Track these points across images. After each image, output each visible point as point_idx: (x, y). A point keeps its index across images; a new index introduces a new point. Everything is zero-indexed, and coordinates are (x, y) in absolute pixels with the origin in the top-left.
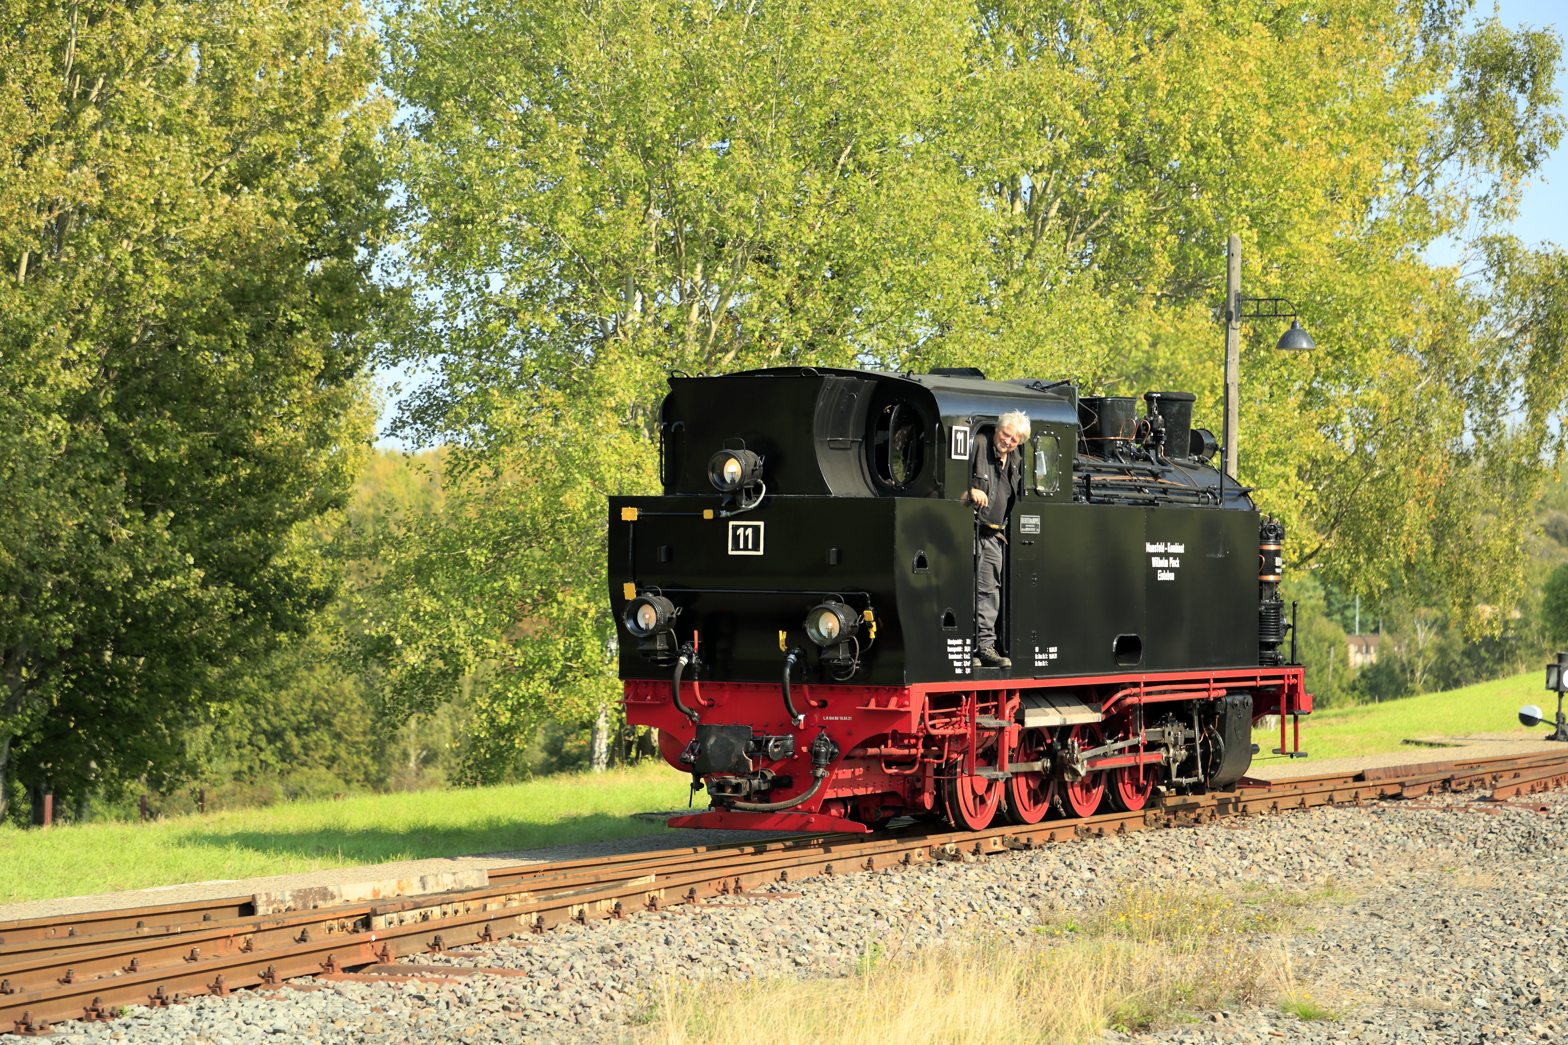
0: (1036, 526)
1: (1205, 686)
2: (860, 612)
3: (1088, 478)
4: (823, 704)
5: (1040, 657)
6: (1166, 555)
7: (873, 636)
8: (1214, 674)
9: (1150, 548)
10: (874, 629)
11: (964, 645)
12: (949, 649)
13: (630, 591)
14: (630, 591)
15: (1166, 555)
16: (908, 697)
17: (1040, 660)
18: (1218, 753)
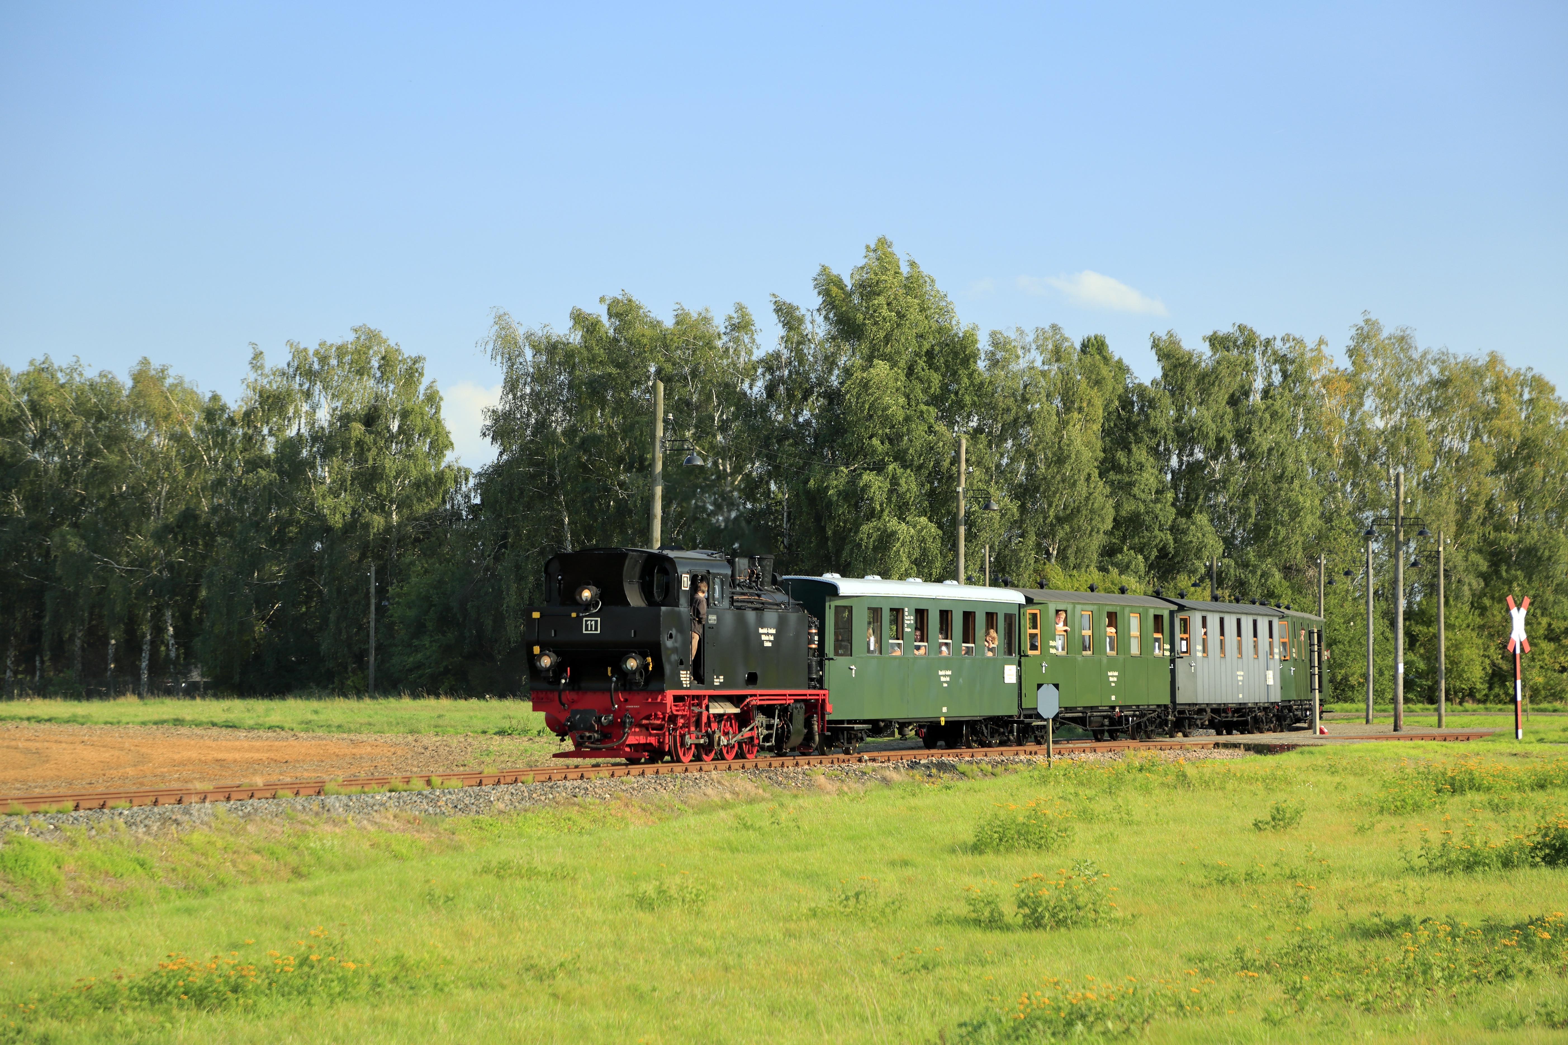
2: (645, 658)
4: (626, 700)
6: (767, 634)
8: (788, 692)
13: (537, 650)
14: (537, 650)
15: (767, 634)
17: (717, 682)
18: (789, 731)
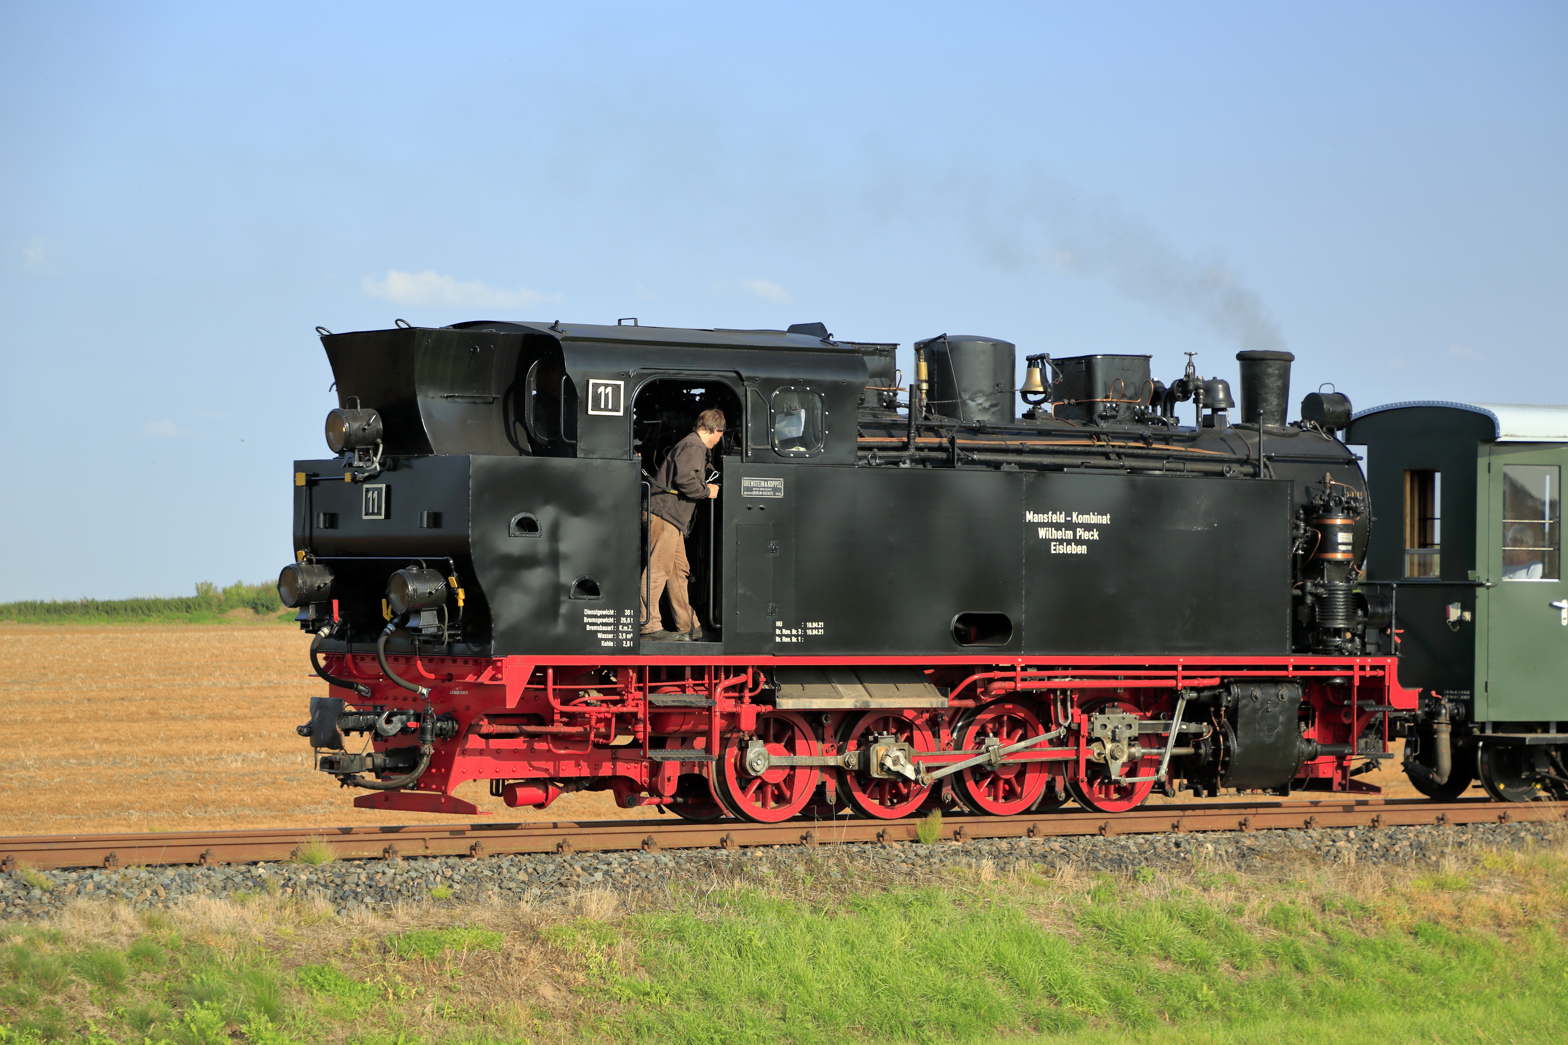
0: (775, 489)
3: (952, 441)
5: (787, 632)
7: (461, 604)
9: (1030, 517)
10: (461, 594)
11: (618, 616)
12: (586, 620)
15: (1070, 526)
16: (499, 670)
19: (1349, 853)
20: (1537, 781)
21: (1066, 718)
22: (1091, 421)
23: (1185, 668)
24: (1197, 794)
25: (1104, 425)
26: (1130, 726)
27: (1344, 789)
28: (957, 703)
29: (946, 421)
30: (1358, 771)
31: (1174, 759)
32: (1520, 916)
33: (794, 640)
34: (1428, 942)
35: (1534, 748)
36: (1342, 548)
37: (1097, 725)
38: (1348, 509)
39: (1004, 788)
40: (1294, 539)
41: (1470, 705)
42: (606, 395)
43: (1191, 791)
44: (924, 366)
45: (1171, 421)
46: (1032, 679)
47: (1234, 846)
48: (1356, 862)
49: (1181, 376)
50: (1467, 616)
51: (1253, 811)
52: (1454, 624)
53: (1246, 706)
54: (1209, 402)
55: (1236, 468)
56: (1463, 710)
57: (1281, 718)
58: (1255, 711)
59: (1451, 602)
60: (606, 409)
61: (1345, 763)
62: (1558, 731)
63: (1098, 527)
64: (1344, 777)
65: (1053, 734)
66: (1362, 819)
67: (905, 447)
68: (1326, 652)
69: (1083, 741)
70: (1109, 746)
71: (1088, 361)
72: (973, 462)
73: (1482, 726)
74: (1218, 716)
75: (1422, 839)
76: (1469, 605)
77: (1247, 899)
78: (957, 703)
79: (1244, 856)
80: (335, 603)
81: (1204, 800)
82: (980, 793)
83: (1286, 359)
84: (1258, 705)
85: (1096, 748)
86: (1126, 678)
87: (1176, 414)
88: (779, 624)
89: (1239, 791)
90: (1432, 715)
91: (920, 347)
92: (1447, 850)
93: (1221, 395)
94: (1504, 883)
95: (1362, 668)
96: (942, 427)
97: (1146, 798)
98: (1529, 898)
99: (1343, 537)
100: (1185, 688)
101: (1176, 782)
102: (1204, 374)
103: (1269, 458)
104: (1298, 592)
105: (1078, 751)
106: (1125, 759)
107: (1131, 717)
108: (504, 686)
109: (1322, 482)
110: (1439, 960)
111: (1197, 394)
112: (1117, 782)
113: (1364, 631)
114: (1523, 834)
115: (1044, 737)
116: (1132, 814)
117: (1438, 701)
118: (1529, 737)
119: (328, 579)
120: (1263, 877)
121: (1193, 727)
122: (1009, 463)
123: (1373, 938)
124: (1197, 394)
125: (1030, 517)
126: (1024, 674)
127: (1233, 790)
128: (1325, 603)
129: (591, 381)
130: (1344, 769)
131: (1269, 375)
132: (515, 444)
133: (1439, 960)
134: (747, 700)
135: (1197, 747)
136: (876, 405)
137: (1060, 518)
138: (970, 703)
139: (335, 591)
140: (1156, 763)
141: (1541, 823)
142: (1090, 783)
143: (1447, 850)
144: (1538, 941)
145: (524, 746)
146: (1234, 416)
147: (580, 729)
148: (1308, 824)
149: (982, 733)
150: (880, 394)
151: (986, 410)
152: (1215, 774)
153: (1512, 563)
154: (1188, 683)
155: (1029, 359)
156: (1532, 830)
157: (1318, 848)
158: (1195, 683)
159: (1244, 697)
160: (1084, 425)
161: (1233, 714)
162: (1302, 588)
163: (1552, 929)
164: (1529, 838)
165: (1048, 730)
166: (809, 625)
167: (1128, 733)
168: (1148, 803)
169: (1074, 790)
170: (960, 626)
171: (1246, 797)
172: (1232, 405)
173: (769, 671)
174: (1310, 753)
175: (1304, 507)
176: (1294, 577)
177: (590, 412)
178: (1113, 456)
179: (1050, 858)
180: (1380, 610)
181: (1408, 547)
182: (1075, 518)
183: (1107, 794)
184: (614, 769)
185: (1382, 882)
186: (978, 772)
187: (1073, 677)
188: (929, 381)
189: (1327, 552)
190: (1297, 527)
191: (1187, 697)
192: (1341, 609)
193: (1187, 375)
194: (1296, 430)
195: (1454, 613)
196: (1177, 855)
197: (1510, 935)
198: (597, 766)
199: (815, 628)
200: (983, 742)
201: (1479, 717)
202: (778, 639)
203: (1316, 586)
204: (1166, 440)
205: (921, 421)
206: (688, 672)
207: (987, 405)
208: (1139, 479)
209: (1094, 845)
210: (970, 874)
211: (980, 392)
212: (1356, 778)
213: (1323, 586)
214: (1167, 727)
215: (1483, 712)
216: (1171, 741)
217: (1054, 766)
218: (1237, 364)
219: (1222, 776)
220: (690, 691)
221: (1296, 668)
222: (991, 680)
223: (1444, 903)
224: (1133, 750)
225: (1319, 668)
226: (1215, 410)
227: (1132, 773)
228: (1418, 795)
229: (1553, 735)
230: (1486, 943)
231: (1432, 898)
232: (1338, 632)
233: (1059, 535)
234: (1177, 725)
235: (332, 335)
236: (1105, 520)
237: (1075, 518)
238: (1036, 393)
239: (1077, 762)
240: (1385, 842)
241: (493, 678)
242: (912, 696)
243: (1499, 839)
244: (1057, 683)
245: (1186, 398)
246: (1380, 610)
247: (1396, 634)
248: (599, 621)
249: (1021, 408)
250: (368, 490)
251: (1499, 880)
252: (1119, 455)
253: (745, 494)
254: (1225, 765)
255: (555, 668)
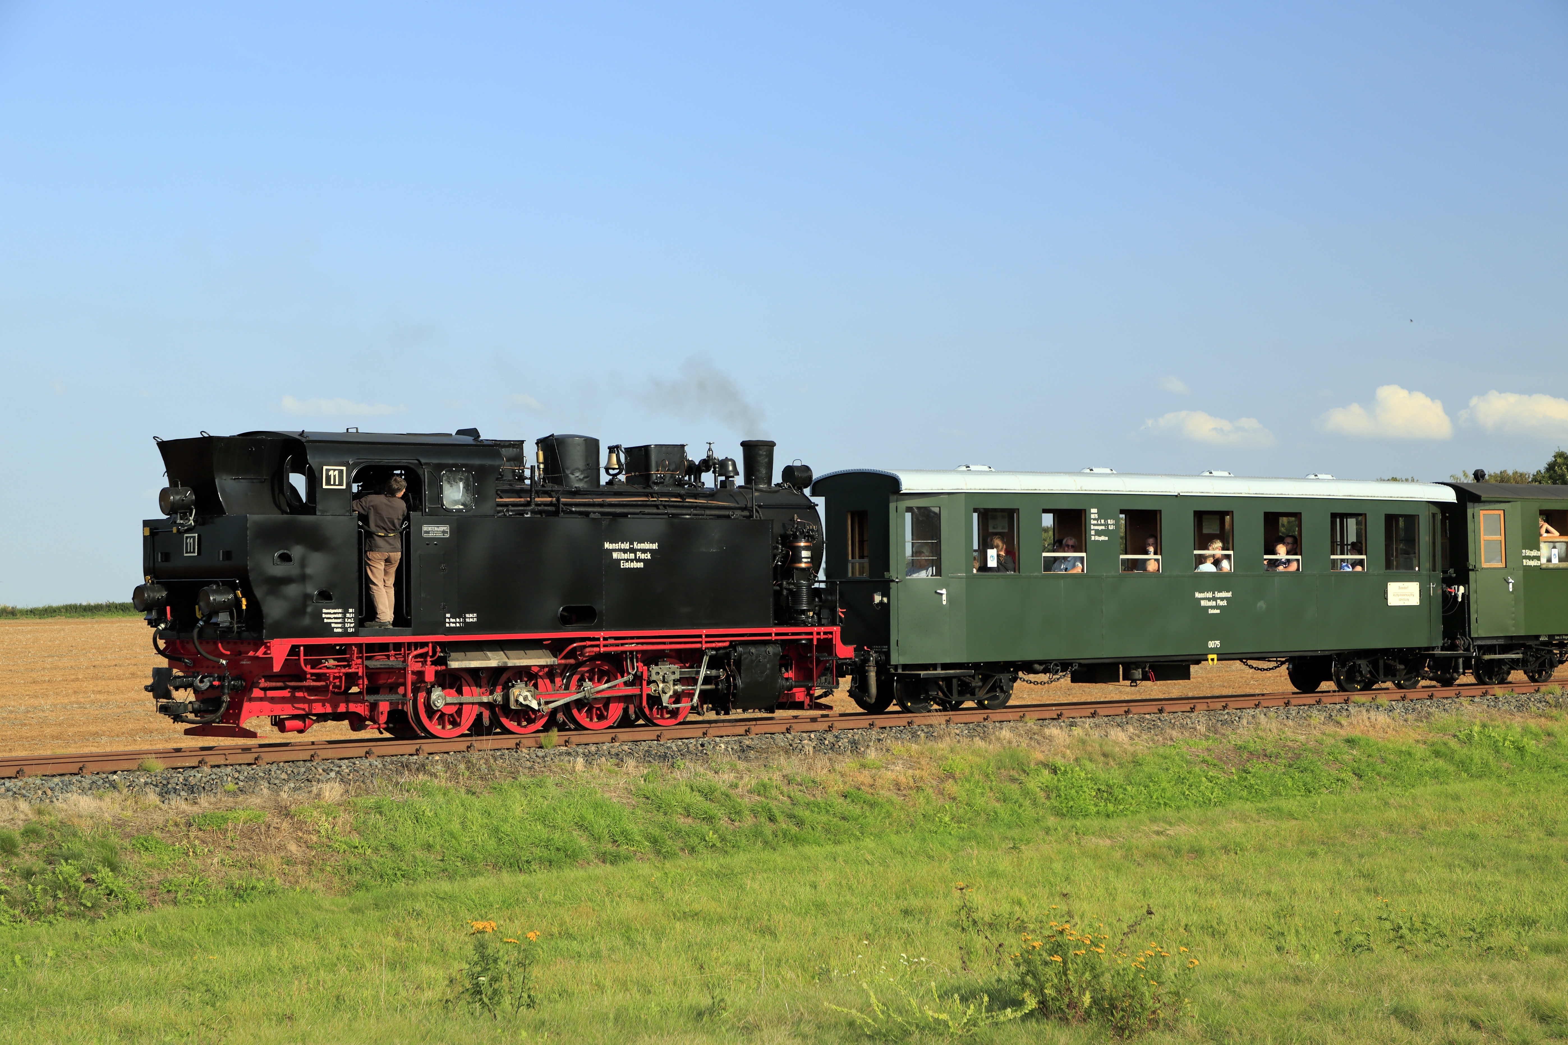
0: (444, 532)
1: (700, 639)
3: (558, 500)
7: (244, 607)
9: (607, 545)
11: (344, 613)
12: (324, 616)
15: (633, 551)
16: (268, 648)
19: (809, 747)
20: (931, 700)
21: (633, 669)
22: (648, 486)
23: (707, 636)
24: (718, 714)
25: (656, 488)
26: (674, 673)
27: (811, 708)
28: (563, 661)
29: (556, 488)
30: (820, 697)
31: (702, 692)
32: (911, 783)
33: (458, 625)
34: (853, 801)
35: (928, 680)
36: (804, 560)
37: (653, 673)
38: (808, 536)
39: (596, 713)
40: (775, 556)
41: (888, 654)
42: (335, 476)
43: (714, 712)
44: (541, 453)
45: (700, 484)
46: (612, 645)
47: (738, 744)
48: (814, 752)
49: (705, 457)
50: (885, 600)
51: (754, 723)
52: (878, 604)
53: (746, 658)
54: (723, 472)
55: (738, 513)
56: (883, 658)
57: (768, 666)
58: (752, 661)
59: (876, 592)
60: (334, 484)
61: (811, 692)
62: (942, 669)
63: (651, 551)
64: (811, 700)
65: (625, 679)
66: (822, 726)
67: (528, 504)
68: (796, 625)
69: (644, 683)
70: (661, 685)
71: (646, 448)
72: (572, 512)
73: (896, 667)
74: (729, 665)
75: (856, 737)
76: (886, 593)
77: (742, 778)
78: (563, 661)
79: (744, 751)
80: (168, 608)
81: (722, 717)
82: (581, 717)
83: (771, 445)
84: (754, 658)
85: (653, 687)
86: (671, 643)
87: (702, 480)
88: (448, 615)
89: (744, 711)
90: (866, 661)
91: (539, 442)
92: (871, 744)
93: (731, 468)
94: (903, 764)
95: (818, 633)
96: (552, 491)
97: (686, 717)
98: (917, 772)
99: (805, 554)
100: (708, 648)
101: (705, 706)
102: (719, 455)
103: (760, 506)
104: (778, 588)
105: (641, 689)
106: (671, 693)
107: (674, 667)
108: (272, 658)
109: (792, 520)
110: (858, 811)
111: (715, 468)
112: (666, 707)
113: (820, 611)
114: (919, 733)
115: (620, 680)
116: (677, 727)
117: (869, 652)
118: (922, 673)
119: (164, 594)
120: (755, 764)
121: (714, 672)
122: (594, 513)
123: (819, 799)
124: (715, 468)
125: (607, 545)
126: (606, 642)
127: (740, 711)
128: (795, 595)
129: (325, 468)
130: (811, 696)
131: (761, 455)
132: (279, 507)
133: (858, 811)
134: (429, 663)
135: (717, 684)
136: (511, 478)
137: (626, 546)
138: (572, 661)
139: (168, 601)
140: (691, 695)
141: (931, 726)
142: (651, 709)
143: (871, 744)
144: (922, 798)
145: (289, 695)
146: (739, 481)
147: (323, 683)
148: (788, 730)
149: (582, 680)
150: (514, 471)
151: (581, 480)
152: (728, 701)
153: (916, 566)
154: (709, 645)
155: (610, 448)
156: (926, 730)
157: (791, 745)
158: (714, 645)
159: (745, 653)
160: (644, 488)
161: (738, 663)
162: (781, 585)
163: (931, 790)
164: (923, 735)
165: (623, 676)
166: (467, 615)
167: (673, 677)
168: (688, 719)
169: (640, 713)
170: (565, 614)
171: (749, 714)
172: (737, 474)
173: (444, 645)
174: (787, 687)
175: (781, 536)
176: (775, 578)
177: (324, 487)
178: (661, 507)
179: (621, 755)
180: (830, 598)
181: (850, 558)
182: (636, 546)
183: (662, 715)
184: (347, 708)
185: (828, 764)
186: (580, 704)
187: (637, 644)
188: (545, 463)
189: (796, 563)
190: (777, 548)
191: (709, 654)
192: (805, 599)
193: (708, 457)
194: (778, 488)
195: (877, 598)
196: (702, 752)
197: (905, 795)
198: (335, 706)
199: (471, 618)
200: (582, 685)
201: (893, 661)
202: (447, 625)
203: (789, 584)
204: (695, 496)
205: (539, 488)
206: (391, 647)
207: (581, 477)
208: (676, 520)
209: (650, 747)
210: (569, 767)
211: (578, 469)
212: (818, 701)
213: (793, 584)
214: (698, 673)
215: (896, 659)
216: (700, 681)
217: (627, 699)
218: (741, 448)
219: (732, 702)
220: (392, 658)
221: (777, 634)
222: (585, 647)
223: (865, 777)
224: (676, 687)
225: (793, 634)
226: (727, 478)
227: (677, 701)
228: (861, 710)
229: (939, 671)
230: (889, 801)
231: (858, 774)
232: (803, 612)
233: (626, 556)
234: (703, 672)
235: (163, 442)
236: (655, 546)
237: (636, 546)
238: (614, 469)
239: (641, 696)
240: (832, 740)
241: (265, 653)
242: (535, 658)
243: (904, 736)
244: (627, 647)
245: (708, 470)
246: (830, 598)
247: (840, 612)
248: (332, 616)
249: (604, 478)
250: (187, 538)
251: (900, 762)
252: (665, 507)
253: (425, 535)
254: (734, 695)
255: (304, 646)
